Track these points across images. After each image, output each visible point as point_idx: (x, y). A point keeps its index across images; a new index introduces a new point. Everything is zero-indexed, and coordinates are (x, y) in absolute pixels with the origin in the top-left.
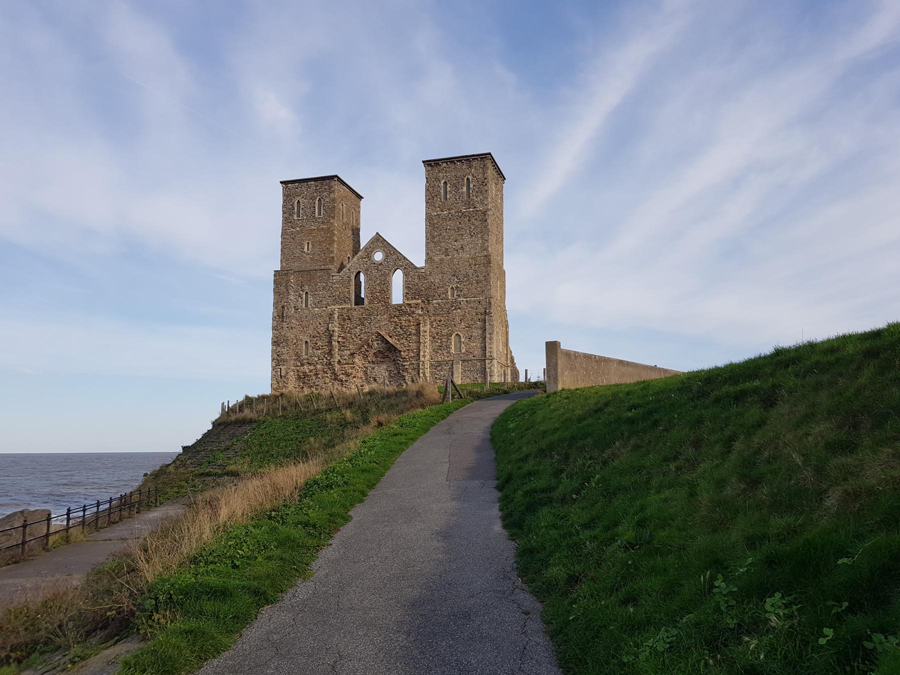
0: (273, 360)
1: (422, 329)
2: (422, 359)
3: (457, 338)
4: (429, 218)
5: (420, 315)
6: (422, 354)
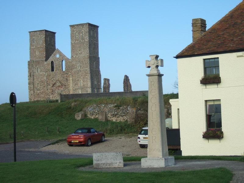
0: (29, 89)
4: (72, 44)
5: (71, 74)
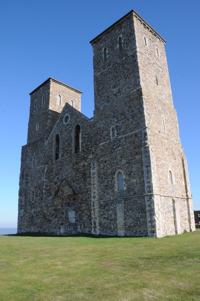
1: (92, 171)
2: (93, 200)
3: (120, 174)
4: (96, 79)
6: (92, 195)
